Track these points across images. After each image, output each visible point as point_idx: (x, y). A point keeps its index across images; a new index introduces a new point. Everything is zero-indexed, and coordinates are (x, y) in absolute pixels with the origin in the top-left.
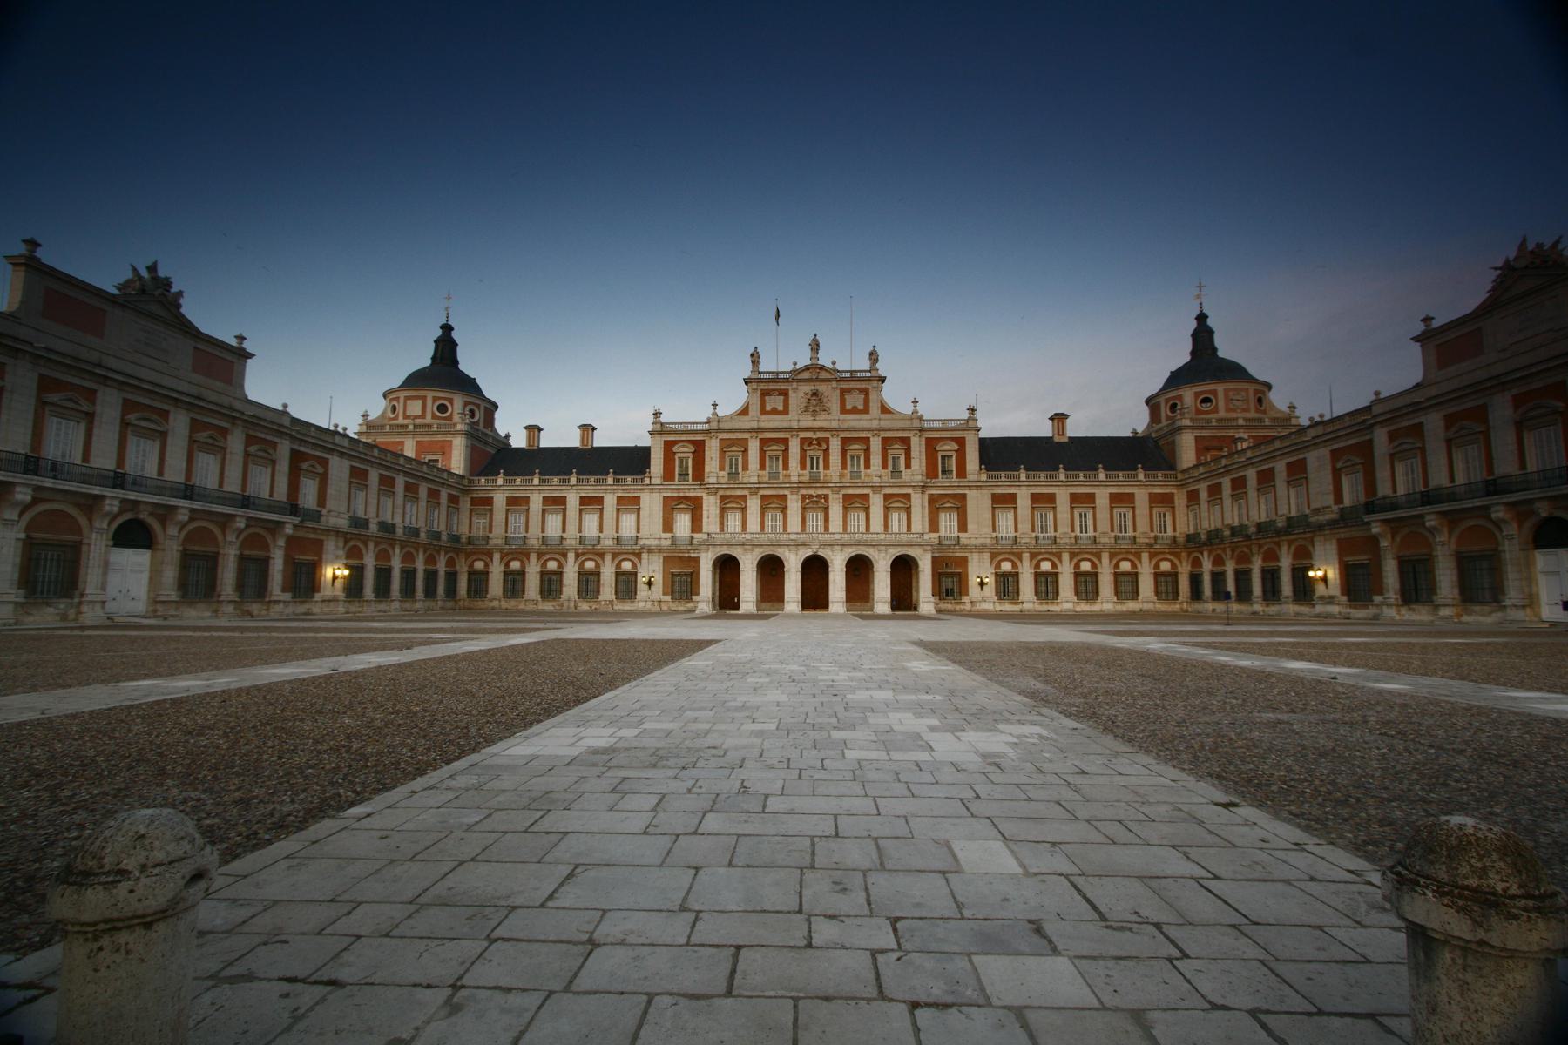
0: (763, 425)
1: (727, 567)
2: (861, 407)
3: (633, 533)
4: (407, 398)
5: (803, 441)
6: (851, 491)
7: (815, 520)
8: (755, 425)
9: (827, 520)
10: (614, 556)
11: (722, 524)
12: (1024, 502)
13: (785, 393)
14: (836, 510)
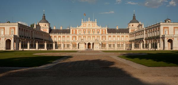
7: (89, 38)
12: (112, 36)
13: (86, 24)
14: (91, 38)
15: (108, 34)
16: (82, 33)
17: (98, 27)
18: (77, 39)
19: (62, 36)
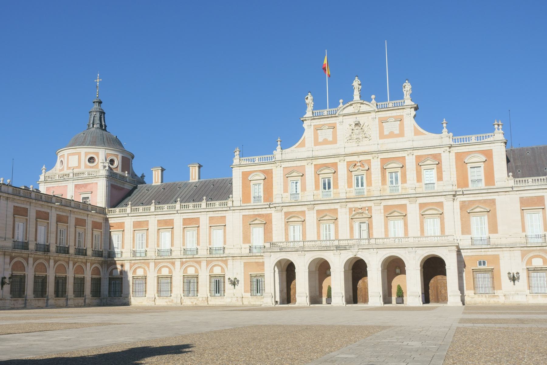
0: (316, 154)
1: (288, 271)
2: (397, 132)
3: (221, 245)
4: (69, 155)
6: (390, 203)
8: (310, 154)
9: (369, 227)
10: (208, 263)
13: (333, 127)
15: (511, 182)
16: (311, 191)
17: (430, 139)
18: (278, 236)
19: (178, 220)
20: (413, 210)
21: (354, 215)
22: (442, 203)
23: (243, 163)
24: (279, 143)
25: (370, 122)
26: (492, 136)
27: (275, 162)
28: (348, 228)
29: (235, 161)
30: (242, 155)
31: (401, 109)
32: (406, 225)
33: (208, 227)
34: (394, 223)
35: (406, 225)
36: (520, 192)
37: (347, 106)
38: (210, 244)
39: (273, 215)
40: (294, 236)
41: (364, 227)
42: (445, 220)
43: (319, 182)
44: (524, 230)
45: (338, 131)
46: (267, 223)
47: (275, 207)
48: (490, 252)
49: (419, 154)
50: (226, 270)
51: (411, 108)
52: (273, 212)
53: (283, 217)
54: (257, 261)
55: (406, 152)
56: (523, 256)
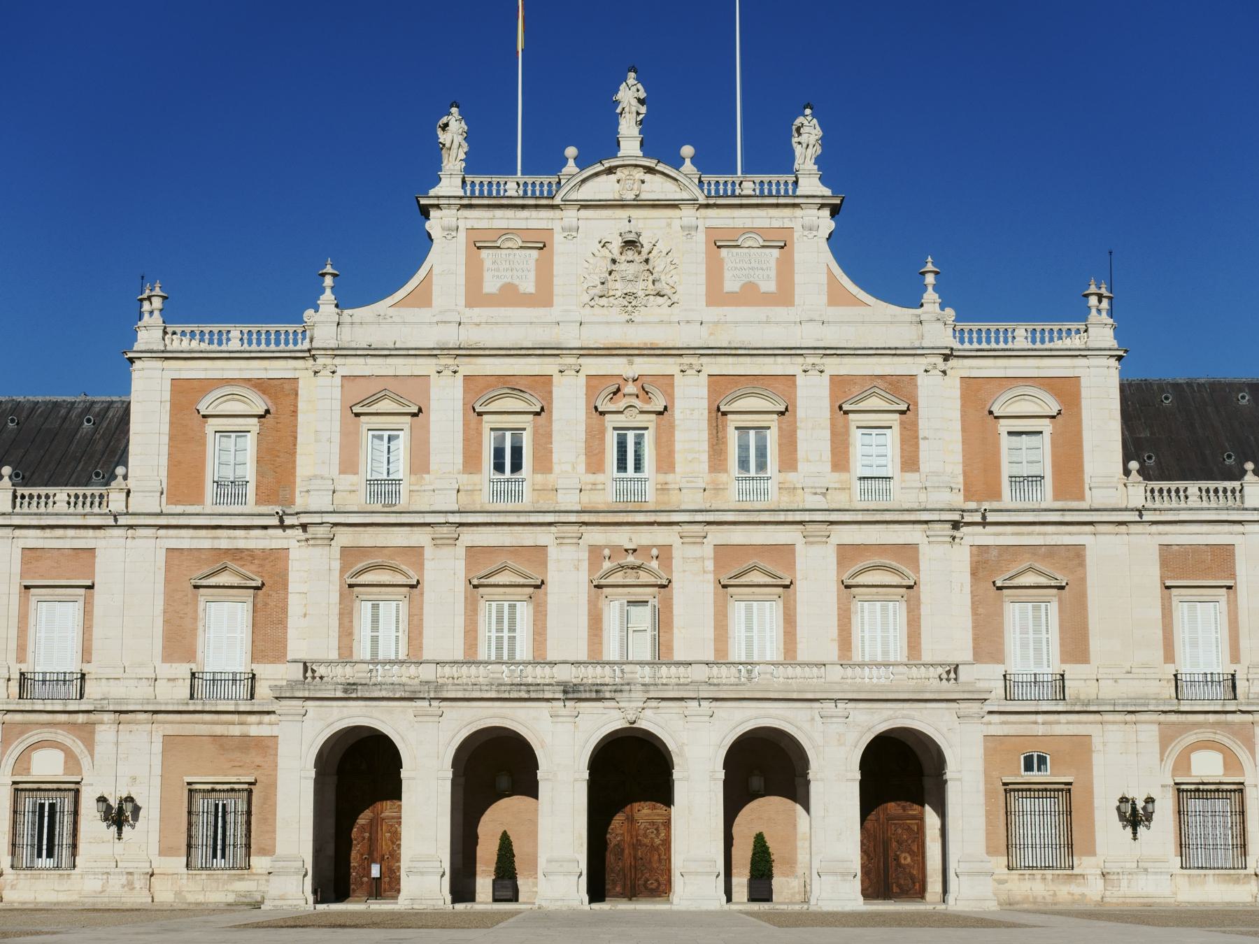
2: (769, 286)
3: (70, 663)
5: (594, 381)
6: (738, 536)
8: (450, 336)
9: (662, 621)
11: (346, 633)
15: (1136, 493)
16: (448, 477)
17: (881, 321)
20: (816, 568)
21: (607, 575)
22: (913, 548)
23: (176, 344)
24: (328, 281)
25: (678, 237)
26: (1078, 331)
27: (311, 354)
28: (584, 620)
29: (142, 335)
30: (169, 316)
31: (786, 205)
32: (790, 620)
33: (16, 589)
34: (749, 611)
35: (790, 620)
36: (1161, 528)
37: (597, 174)
38: (21, 659)
39: (293, 554)
40: (375, 640)
41: (642, 617)
42: (925, 610)
43: (480, 444)
44: (1169, 657)
45: (557, 260)
46: (265, 588)
47: (304, 527)
48: (1065, 726)
49: (843, 371)
50: (85, 761)
51: (822, 206)
52: (293, 544)
53: (336, 565)
54: (219, 730)
55: (800, 360)
56: (1165, 742)
